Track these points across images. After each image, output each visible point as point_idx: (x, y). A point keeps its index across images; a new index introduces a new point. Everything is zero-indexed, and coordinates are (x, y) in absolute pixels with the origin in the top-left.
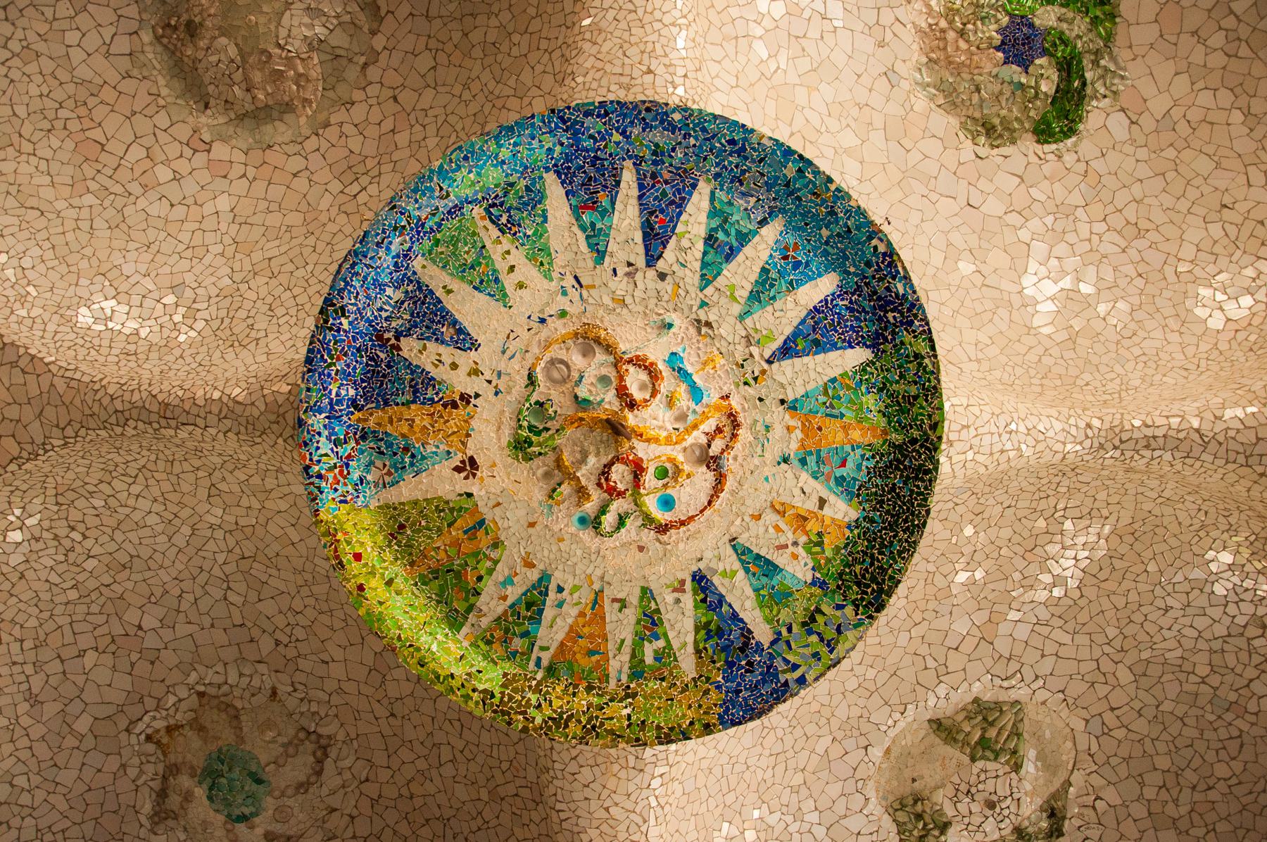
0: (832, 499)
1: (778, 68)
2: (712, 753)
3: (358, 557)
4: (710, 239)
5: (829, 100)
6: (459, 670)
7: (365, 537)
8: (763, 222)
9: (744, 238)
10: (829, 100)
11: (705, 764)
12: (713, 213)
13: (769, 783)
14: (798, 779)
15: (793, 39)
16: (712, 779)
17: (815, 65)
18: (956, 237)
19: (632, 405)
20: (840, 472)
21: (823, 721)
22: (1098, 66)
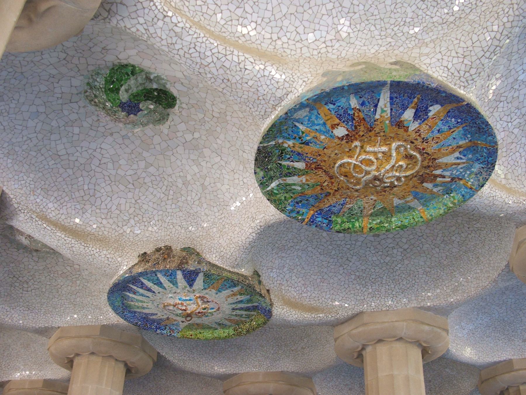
0: (233, 289)
1: (109, 176)
2: (299, 267)
3: (191, 335)
4: (155, 284)
5: (126, 163)
6: (225, 335)
7: (188, 333)
8: (156, 275)
9: (158, 279)
10: (126, 163)
11: (300, 269)
12: (149, 280)
13: (322, 251)
14: (328, 243)
15: (100, 166)
16: (306, 268)
17: (111, 161)
18: (192, 157)
19: (185, 310)
20: (227, 286)
21: (317, 234)
22: (152, 80)
